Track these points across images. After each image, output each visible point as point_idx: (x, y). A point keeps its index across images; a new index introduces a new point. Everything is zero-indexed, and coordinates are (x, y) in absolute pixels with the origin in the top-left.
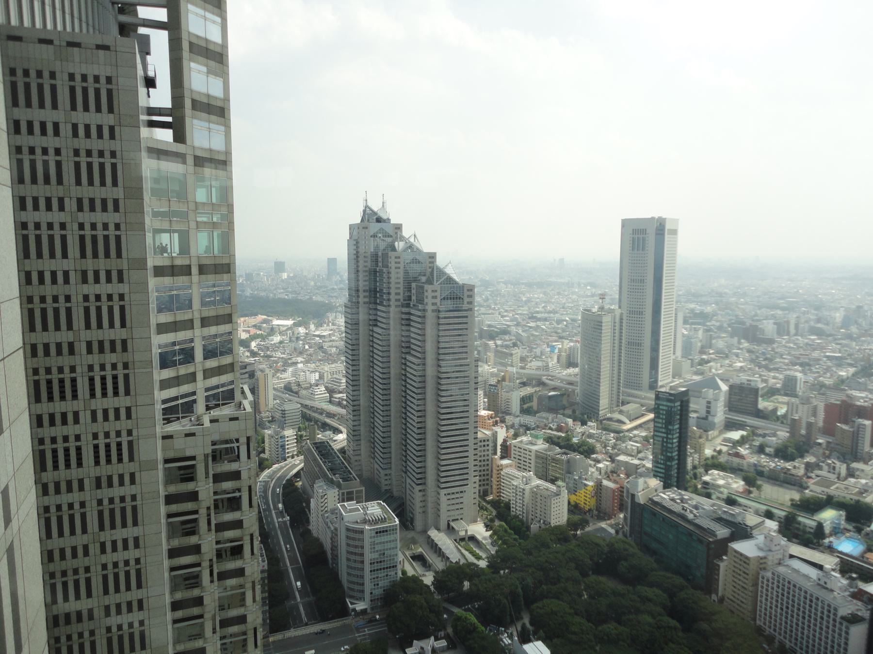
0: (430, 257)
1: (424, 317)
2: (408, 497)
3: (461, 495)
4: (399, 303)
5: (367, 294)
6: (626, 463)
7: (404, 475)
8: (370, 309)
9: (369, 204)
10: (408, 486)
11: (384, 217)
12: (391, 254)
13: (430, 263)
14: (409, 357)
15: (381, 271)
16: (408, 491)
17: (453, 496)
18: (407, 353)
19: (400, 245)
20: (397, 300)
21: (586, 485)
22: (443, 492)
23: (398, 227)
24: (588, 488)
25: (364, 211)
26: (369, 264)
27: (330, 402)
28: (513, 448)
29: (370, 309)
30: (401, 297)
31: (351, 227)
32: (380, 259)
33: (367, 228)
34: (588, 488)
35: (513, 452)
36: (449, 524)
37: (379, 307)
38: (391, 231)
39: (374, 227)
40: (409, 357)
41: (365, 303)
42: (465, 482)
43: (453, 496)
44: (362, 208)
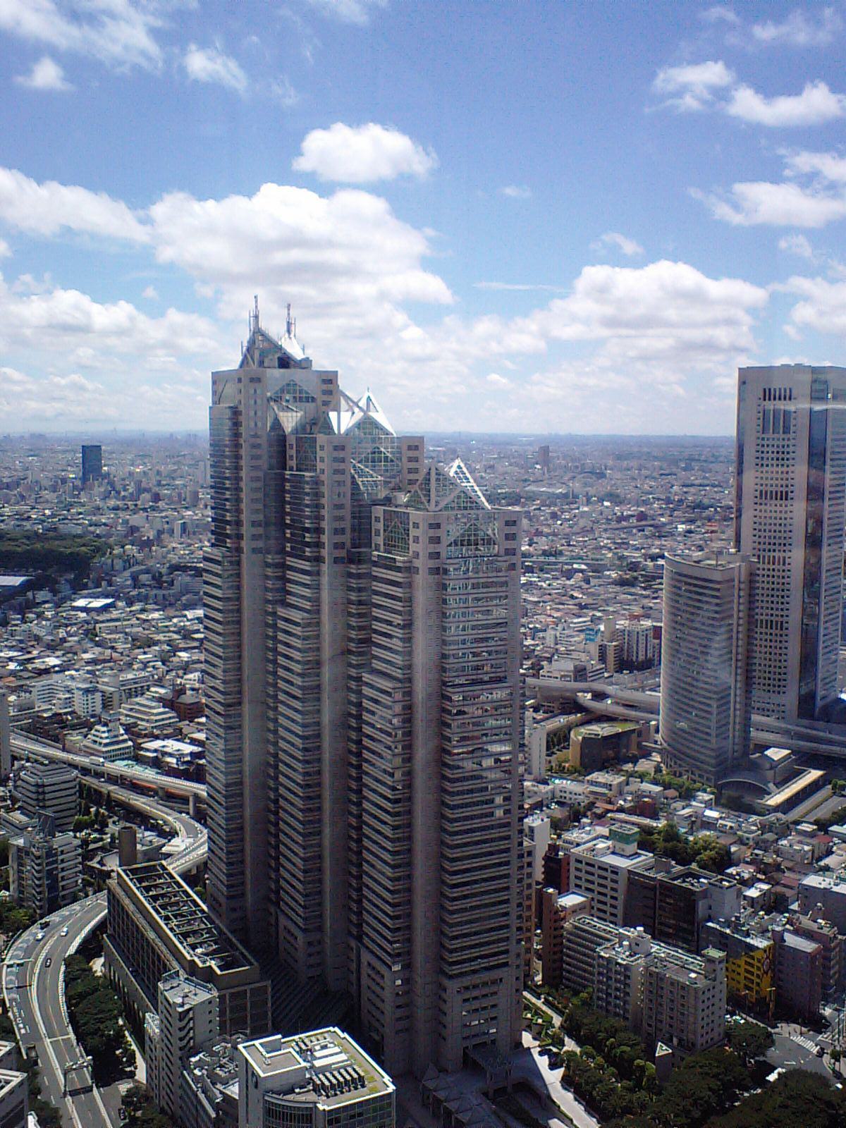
0: (410, 448)
1: (410, 585)
2: (366, 994)
3: (493, 989)
4: (343, 553)
5: (260, 530)
6: (826, 892)
7: (353, 943)
8: (267, 565)
9: (263, 325)
10: (365, 970)
11: (296, 352)
12: (321, 439)
13: (410, 460)
14: (367, 677)
15: (298, 481)
16: (365, 981)
17: (476, 993)
18: (358, 666)
19: (342, 421)
20: (338, 546)
21: (752, 948)
22: (452, 986)
23: (329, 380)
24: (757, 955)
25: (252, 342)
26: (264, 463)
27: (138, 759)
28: (573, 865)
29: (267, 565)
30: (346, 538)
31: (218, 379)
32: (292, 452)
33: (259, 380)
34: (757, 955)
35: (573, 873)
36: (465, 1054)
37: (291, 561)
38: (313, 388)
39: (276, 375)
40: (367, 677)
41: (254, 550)
42: (502, 959)
43: (476, 993)
44: (246, 336)
